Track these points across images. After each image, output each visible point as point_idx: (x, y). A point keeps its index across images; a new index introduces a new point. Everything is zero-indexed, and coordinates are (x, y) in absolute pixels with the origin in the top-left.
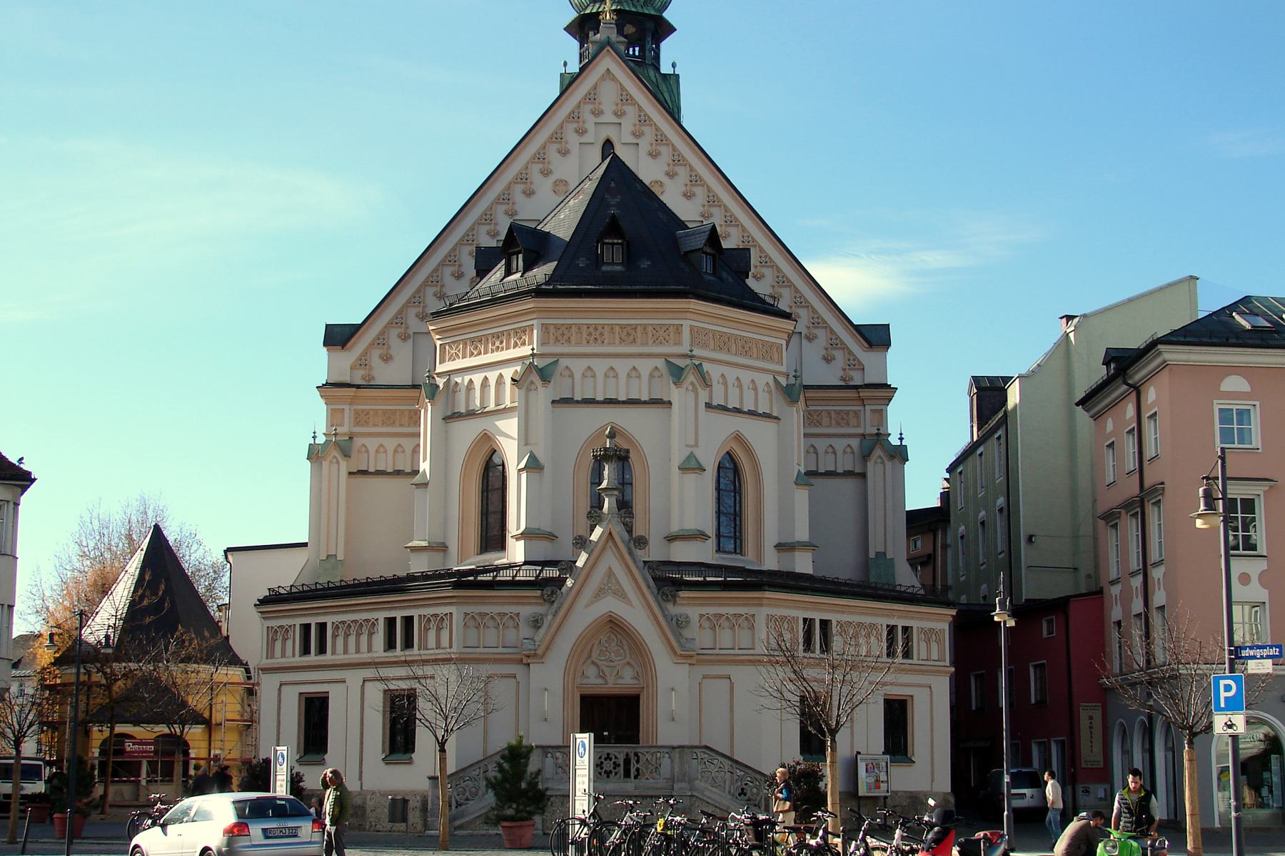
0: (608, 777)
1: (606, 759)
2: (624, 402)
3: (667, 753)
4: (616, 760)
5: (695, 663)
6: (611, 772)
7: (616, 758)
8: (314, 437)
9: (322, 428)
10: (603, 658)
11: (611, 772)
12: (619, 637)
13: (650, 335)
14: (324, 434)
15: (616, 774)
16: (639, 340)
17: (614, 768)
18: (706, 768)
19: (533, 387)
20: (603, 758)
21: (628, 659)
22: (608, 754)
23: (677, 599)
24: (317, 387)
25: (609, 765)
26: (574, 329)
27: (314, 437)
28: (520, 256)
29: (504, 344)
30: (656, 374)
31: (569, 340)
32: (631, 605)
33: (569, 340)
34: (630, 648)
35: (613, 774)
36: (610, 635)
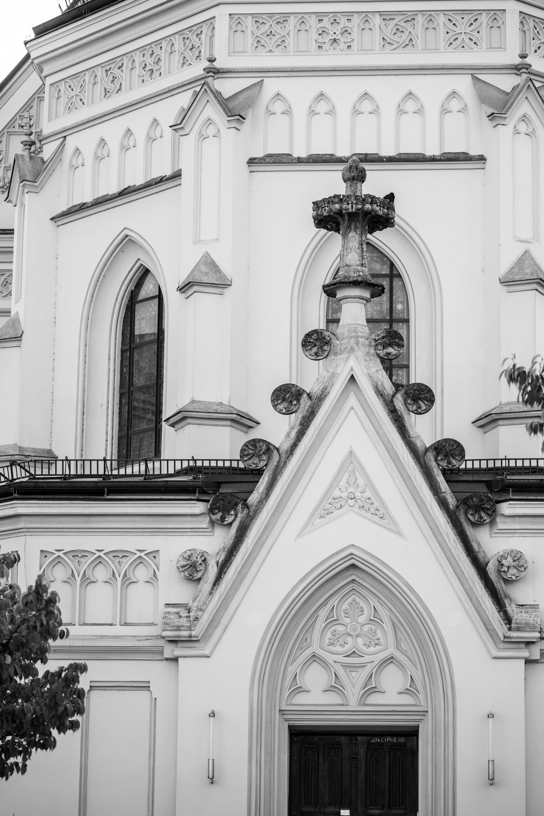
2: (391, 160)
5: (537, 656)
10: (338, 649)
12: (374, 602)
13: (442, 30)
16: (419, 43)
21: (391, 650)
23: (498, 519)
26: (292, 21)
30: (454, 105)
31: (282, 43)
33: (282, 43)
36: (354, 600)
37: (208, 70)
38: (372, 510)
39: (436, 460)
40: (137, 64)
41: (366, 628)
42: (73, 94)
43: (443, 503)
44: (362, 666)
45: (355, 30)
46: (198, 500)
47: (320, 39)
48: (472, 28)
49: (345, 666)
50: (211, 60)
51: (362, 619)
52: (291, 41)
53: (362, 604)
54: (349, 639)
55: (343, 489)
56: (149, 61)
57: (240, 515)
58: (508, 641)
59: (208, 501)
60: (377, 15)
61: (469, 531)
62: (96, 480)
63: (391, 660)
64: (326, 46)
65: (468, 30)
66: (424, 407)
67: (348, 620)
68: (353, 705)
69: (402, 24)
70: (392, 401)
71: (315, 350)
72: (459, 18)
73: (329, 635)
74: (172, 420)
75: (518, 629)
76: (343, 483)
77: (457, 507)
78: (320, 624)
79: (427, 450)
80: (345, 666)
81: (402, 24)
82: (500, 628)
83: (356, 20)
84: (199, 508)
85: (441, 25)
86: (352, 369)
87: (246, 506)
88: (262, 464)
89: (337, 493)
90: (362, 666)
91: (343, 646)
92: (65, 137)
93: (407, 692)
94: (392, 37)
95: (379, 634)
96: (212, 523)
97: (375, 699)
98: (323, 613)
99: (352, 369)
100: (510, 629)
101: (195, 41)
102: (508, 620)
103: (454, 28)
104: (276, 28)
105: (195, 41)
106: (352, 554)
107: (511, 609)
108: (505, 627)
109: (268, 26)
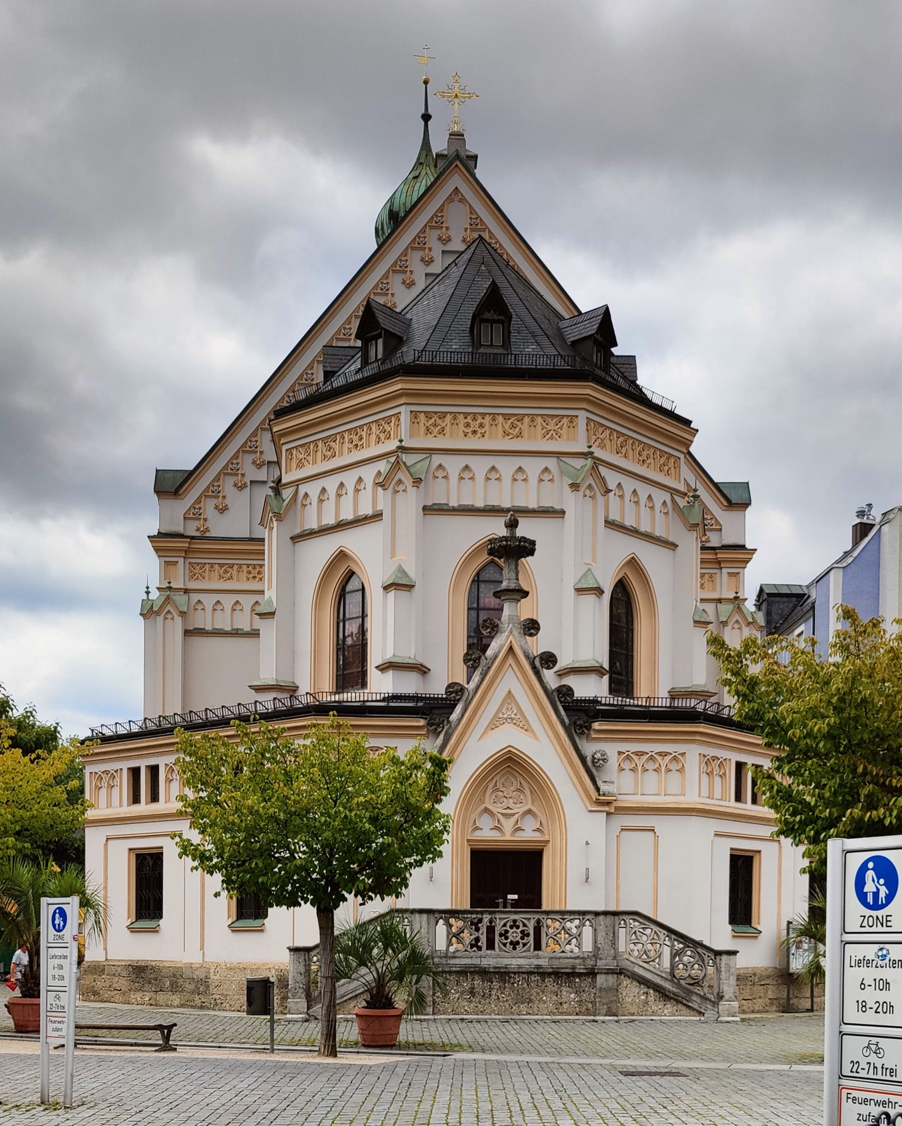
0: (514, 949)
1: (511, 927)
3: (588, 920)
4: (525, 928)
5: (613, 810)
6: (518, 943)
7: (524, 925)
8: (148, 593)
9: (155, 581)
11: (518, 943)
12: (520, 778)
13: (539, 427)
14: (158, 588)
15: (524, 945)
16: (525, 434)
17: (522, 938)
18: (637, 938)
19: (401, 488)
20: (508, 925)
21: (529, 806)
22: (515, 921)
24: (149, 537)
25: (515, 935)
27: (148, 593)
28: (380, 342)
29: (364, 441)
31: (442, 431)
32: (536, 738)
33: (442, 431)
34: (531, 792)
35: (521, 945)
37: (399, 448)
38: (521, 725)
39: (558, 697)
40: (346, 440)
41: (515, 793)
42: (302, 456)
43: (562, 722)
44: (513, 815)
45: (487, 425)
46: (421, 718)
47: (466, 431)
48: (558, 426)
49: (503, 814)
50: (401, 441)
51: (512, 788)
52: (447, 429)
53: (512, 779)
54: (505, 800)
55: (504, 712)
56: (355, 438)
57: (445, 727)
58: (599, 803)
59: (426, 719)
60: (501, 416)
61: (577, 739)
62: (358, 704)
63: (529, 812)
64: (470, 435)
65: (555, 428)
66: (551, 666)
67: (503, 789)
68: (508, 837)
69: (515, 422)
70: (533, 662)
71: (489, 630)
72: (550, 420)
73: (494, 797)
74: (381, 667)
75: (604, 795)
76: (504, 711)
77: (570, 724)
78: (489, 791)
79: (553, 691)
80: (503, 814)
81: (515, 422)
82: (594, 795)
83: (488, 418)
84: (422, 722)
85: (539, 424)
86: (511, 642)
87: (449, 722)
88: (458, 697)
89: (501, 715)
90: (513, 815)
91: (501, 803)
92: (298, 485)
93: (538, 830)
94: (510, 431)
95: (522, 797)
96: (428, 731)
97: (520, 833)
98: (491, 785)
99: (511, 642)
100: (599, 795)
101: (387, 427)
102: (598, 789)
103: (546, 426)
104: (439, 421)
105: (387, 427)
106: (510, 751)
107: (600, 783)
108: (597, 794)
109: (433, 420)
